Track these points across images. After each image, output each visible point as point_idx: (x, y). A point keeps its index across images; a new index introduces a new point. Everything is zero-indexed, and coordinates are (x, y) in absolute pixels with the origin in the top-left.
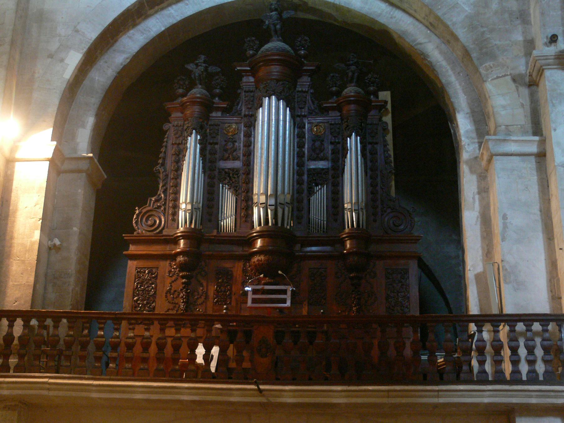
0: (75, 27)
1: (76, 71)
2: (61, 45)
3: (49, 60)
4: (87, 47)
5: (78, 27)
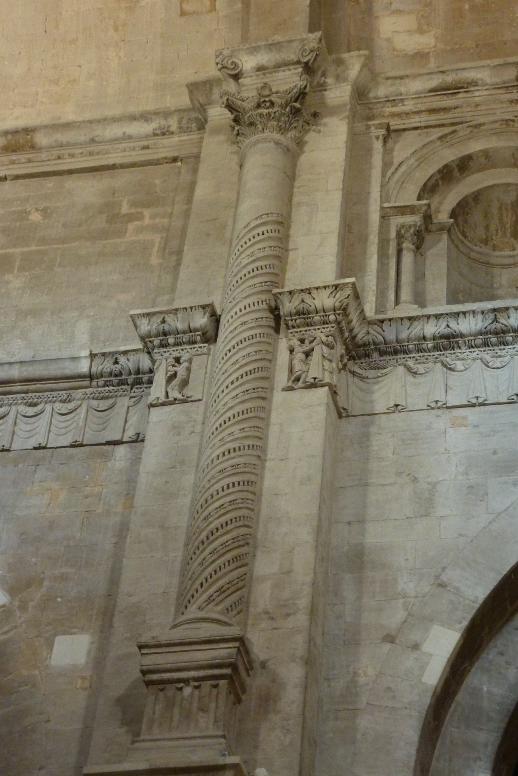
0: (437, 577)
1: (448, 669)
2: (410, 615)
3: (387, 647)
4: (469, 617)
5: (444, 578)
